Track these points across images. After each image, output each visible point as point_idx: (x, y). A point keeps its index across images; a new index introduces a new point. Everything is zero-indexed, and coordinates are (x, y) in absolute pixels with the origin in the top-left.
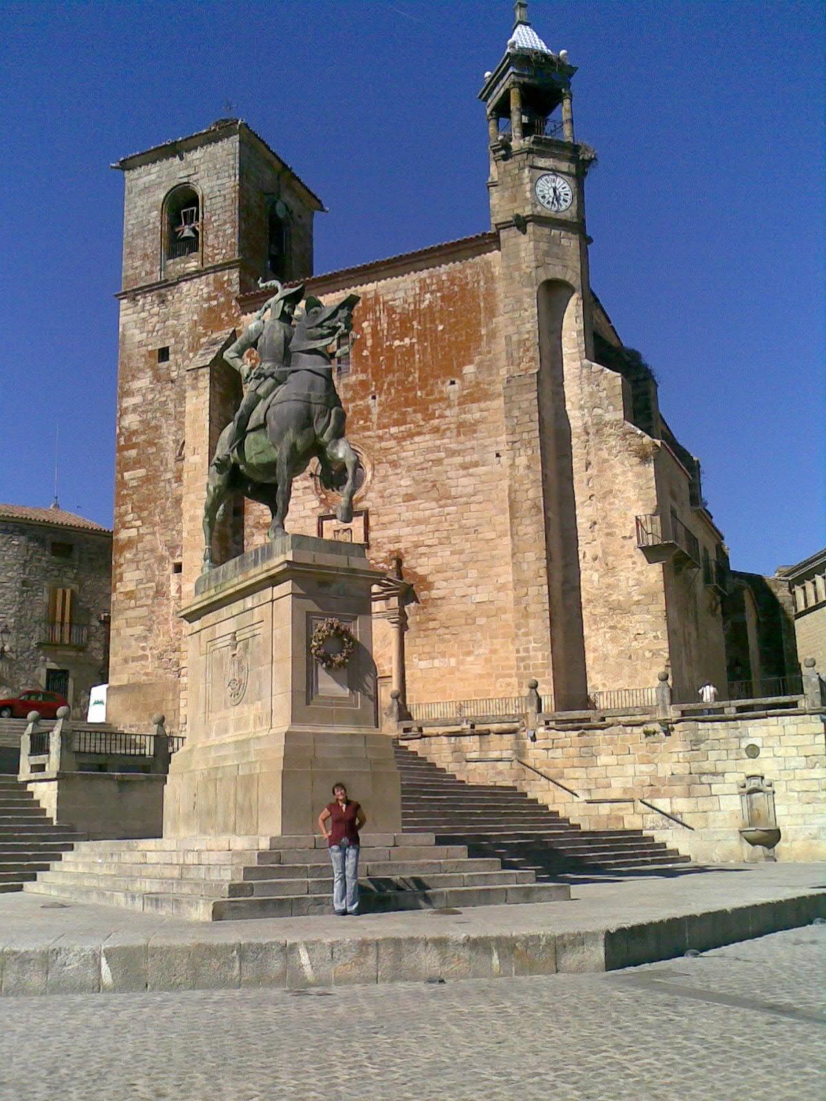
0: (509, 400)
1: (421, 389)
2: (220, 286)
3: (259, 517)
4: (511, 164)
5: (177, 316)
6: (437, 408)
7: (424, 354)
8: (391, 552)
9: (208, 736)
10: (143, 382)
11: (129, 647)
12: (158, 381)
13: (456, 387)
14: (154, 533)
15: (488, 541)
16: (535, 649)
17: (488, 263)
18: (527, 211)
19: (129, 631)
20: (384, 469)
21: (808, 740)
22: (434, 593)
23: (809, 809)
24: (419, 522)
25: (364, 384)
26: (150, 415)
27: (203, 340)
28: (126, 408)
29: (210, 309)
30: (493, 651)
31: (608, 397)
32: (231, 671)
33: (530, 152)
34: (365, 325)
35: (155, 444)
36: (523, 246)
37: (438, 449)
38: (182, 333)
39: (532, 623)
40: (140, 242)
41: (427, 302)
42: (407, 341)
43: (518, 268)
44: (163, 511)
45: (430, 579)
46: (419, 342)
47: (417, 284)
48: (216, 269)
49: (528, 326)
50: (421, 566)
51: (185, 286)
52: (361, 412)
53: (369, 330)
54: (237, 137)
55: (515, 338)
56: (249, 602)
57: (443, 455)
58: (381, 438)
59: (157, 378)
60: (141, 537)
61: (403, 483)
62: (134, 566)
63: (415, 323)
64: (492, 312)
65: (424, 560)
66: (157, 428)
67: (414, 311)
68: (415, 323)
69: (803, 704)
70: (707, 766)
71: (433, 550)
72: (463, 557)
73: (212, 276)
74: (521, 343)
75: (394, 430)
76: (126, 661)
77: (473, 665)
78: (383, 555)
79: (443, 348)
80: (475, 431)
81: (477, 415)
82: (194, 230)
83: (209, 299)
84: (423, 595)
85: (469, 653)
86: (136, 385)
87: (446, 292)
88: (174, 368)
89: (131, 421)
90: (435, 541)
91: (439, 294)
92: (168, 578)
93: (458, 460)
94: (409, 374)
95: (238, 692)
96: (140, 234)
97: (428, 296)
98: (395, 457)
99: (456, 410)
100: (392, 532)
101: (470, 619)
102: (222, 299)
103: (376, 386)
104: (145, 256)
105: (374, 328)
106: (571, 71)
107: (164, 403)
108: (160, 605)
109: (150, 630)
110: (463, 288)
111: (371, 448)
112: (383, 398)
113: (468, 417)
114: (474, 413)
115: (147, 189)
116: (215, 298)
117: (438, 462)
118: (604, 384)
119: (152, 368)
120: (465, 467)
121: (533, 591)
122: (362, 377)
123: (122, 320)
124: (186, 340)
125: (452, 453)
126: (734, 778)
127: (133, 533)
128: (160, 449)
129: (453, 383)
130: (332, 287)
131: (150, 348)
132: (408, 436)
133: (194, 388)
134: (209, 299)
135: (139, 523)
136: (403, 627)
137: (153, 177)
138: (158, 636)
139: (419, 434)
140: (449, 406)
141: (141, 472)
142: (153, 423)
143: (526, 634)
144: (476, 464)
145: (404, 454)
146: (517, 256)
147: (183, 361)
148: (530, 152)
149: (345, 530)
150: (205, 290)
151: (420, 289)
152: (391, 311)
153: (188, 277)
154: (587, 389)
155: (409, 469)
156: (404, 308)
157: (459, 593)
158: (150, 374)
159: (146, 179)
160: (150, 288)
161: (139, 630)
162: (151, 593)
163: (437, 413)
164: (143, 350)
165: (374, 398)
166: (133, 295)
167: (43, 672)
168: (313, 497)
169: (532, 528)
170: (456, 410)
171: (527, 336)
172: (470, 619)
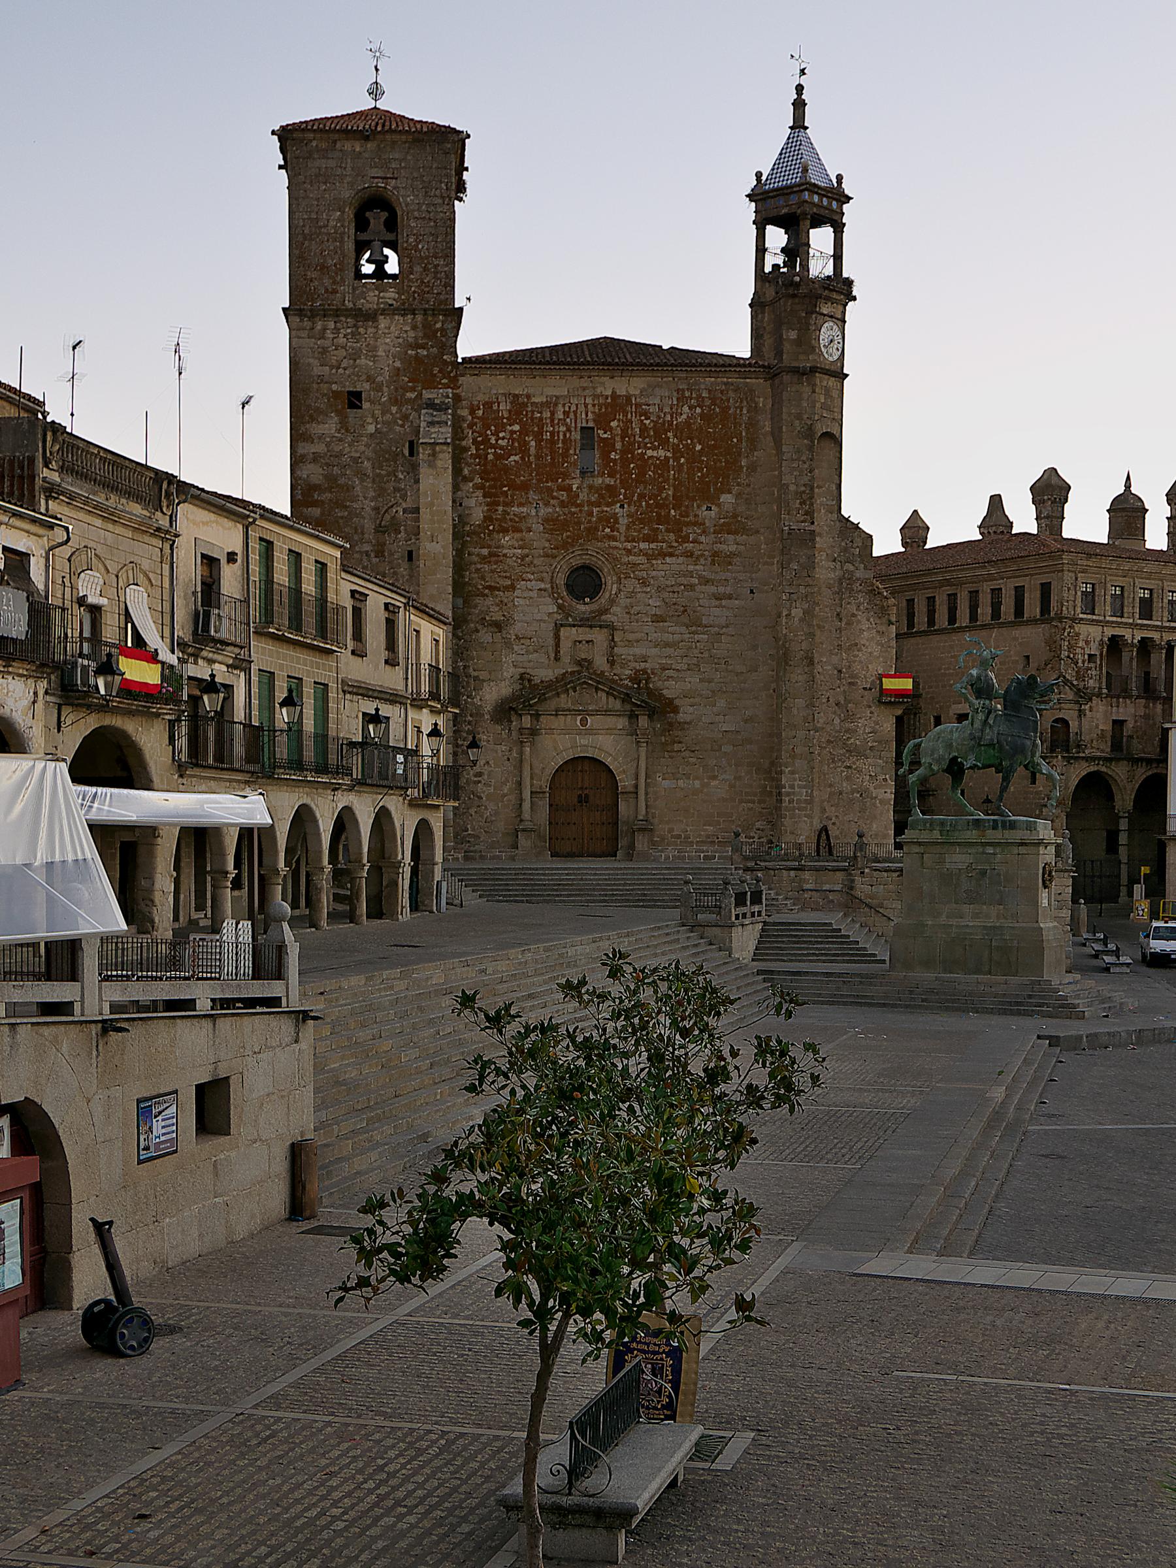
2: (429, 332)
6: (692, 532)
15: (737, 674)
16: (800, 787)
20: (630, 584)
22: (681, 717)
24: (667, 645)
28: (303, 456)
34: (614, 424)
35: (346, 507)
36: (805, 396)
38: (380, 379)
39: (798, 763)
41: (684, 416)
45: (677, 702)
47: (675, 394)
51: (383, 322)
58: (629, 552)
59: (344, 426)
66: (349, 488)
75: (643, 545)
78: (628, 672)
80: (730, 563)
81: (733, 548)
83: (418, 346)
85: (714, 778)
86: (316, 429)
88: (370, 420)
89: (314, 473)
91: (698, 410)
93: (713, 589)
100: (638, 651)
103: (625, 494)
104: (323, 268)
107: (355, 460)
112: (633, 509)
114: (729, 545)
117: (691, 587)
120: (718, 597)
122: (609, 481)
124: (385, 389)
125: (707, 582)
129: (709, 509)
131: (334, 387)
132: (659, 554)
133: (432, 465)
139: (671, 555)
142: (342, 481)
143: (792, 772)
147: (383, 414)
149: (588, 642)
150: (412, 334)
151: (678, 399)
153: (389, 311)
155: (659, 589)
156: (659, 417)
165: (622, 506)
171: (803, 489)
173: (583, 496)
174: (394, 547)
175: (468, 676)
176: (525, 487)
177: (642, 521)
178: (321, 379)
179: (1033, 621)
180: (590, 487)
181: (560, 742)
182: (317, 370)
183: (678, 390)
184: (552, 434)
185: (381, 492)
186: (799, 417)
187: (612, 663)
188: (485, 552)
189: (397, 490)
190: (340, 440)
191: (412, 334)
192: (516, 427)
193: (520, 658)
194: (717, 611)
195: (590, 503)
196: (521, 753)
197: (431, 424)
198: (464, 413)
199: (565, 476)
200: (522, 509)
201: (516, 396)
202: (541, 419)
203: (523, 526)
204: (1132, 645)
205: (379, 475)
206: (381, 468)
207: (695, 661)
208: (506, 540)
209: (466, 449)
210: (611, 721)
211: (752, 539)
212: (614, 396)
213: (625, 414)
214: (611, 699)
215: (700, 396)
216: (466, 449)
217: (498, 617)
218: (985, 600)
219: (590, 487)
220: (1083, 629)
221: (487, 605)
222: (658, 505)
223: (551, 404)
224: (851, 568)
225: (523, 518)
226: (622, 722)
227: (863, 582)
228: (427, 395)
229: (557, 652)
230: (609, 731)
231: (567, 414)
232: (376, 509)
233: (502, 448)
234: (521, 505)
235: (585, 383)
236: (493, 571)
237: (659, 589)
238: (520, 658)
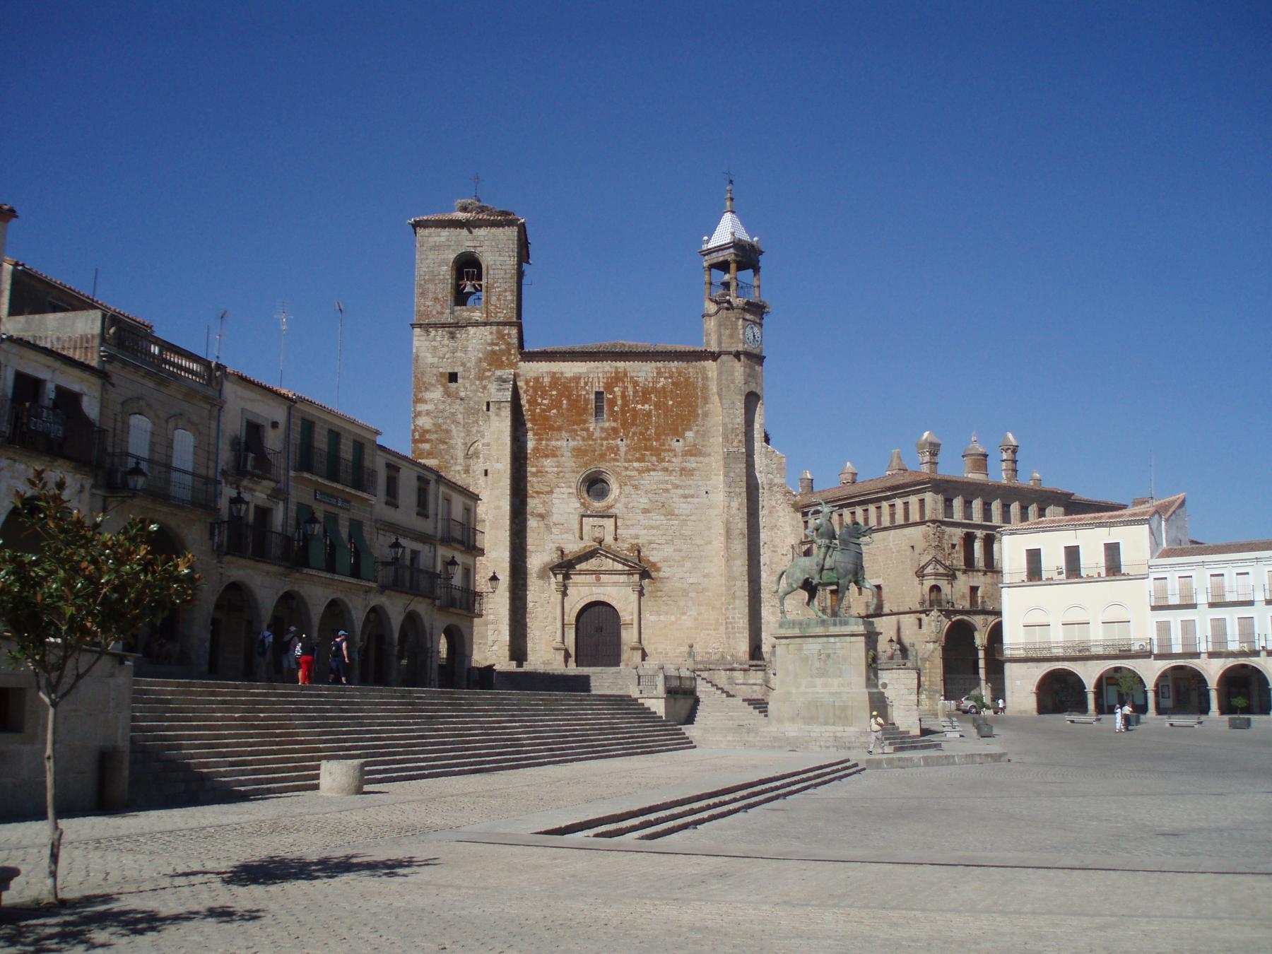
0: (726, 466)
2: (501, 336)
4: (731, 314)
5: (466, 352)
7: (658, 416)
8: (633, 545)
10: (436, 394)
13: (681, 443)
17: (704, 368)
18: (740, 348)
20: (628, 489)
22: (661, 574)
24: (652, 528)
25: (615, 430)
27: (488, 374)
29: (493, 352)
30: (700, 614)
32: (817, 664)
33: (743, 309)
37: (667, 482)
39: (737, 602)
40: (431, 287)
42: (647, 406)
43: (733, 382)
45: (659, 565)
46: (656, 409)
48: (498, 324)
49: (738, 420)
50: (653, 556)
51: (472, 330)
54: (516, 229)
55: (730, 426)
56: (832, 640)
57: (670, 487)
58: (626, 469)
64: (706, 400)
65: (655, 552)
66: (447, 431)
67: (653, 388)
69: (909, 664)
72: (682, 554)
73: (494, 328)
74: (733, 429)
75: (636, 464)
77: (687, 621)
81: (694, 465)
82: (474, 286)
83: (492, 344)
84: (654, 574)
85: (684, 614)
86: (428, 395)
89: (425, 422)
93: (680, 492)
94: (647, 429)
95: (823, 673)
96: (431, 281)
99: (679, 459)
100: (633, 532)
101: (685, 593)
104: (436, 299)
105: (623, 393)
106: (761, 253)
107: (453, 414)
110: (687, 379)
111: (618, 474)
113: (688, 465)
114: (692, 463)
115: (437, 248)
116: (497, 344)
117: (667, 491)
118: (775, 460)
119: (443, 385)
120: (685, 497)
121: (739, 583)
123: (416, 343)
125: (677, 487)
134: (492, 344)
136: (641, 594)
137: (443, 239)
142: (444, 427)
144: (692, 496)
148: (743, 309)
150: (489, 337)
152: (636, 384)
153: (477, 324)
154: (765, 461)
155: (646, 492)
157: (678, 576)
158: (441, 389)
159: (437, 239)
160: (443, 326)
164: (435, 371)
166: (426, 327)
168: (574, 500)
169: (740, 546)
170: (679, 459)
172: (685, 593)
173: (597, 434)
176: (559, 429)
181: (582, 591)
182: (431, 360)
185: (469, 433)
187: (616, 539)
188: (534, 470)
189: (478, 432)
191: (489, 337)
194: (684, 506)
195: (602, 439)
197: (499, 390)
199: (585, 422)
201: (555, 373)
203: (558, 453)
208: (548, 463)
211: (706, 460)
212: (617, 373)
217: (542, 511)
219: (602, 429)
223: (577, 379)
225: (558, 448)
227: (781, 486)
228: (498, 373)
230: (615, 584)
231: (586, 384)
232: (465, 444)
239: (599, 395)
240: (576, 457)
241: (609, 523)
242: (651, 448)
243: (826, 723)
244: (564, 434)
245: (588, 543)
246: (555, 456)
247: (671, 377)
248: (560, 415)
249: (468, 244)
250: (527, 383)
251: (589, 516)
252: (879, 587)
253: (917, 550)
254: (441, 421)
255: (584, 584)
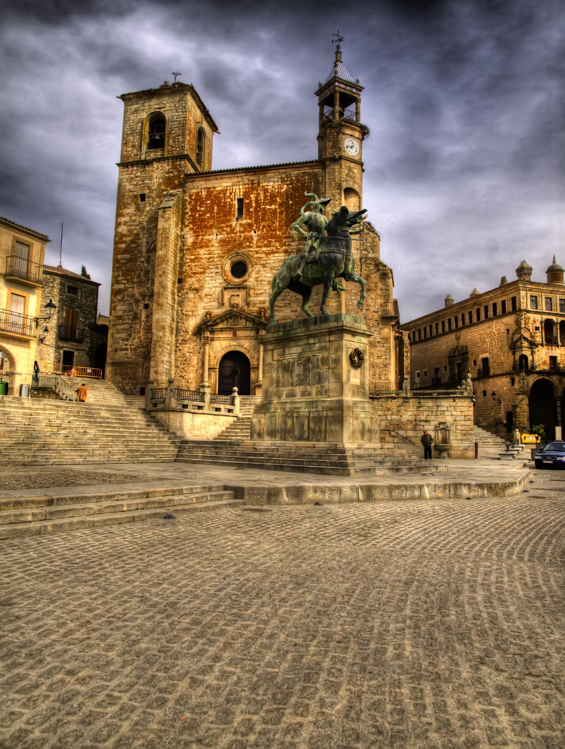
1: (279, 231)
2: (174, 167)
3: (192, 285)
5: (151, 178)
8: (260, 308)
9: (280, 398)
10: (131, 210)
11: (118, 343)
12: (139, 211)
14: (133, 288)
19: (118, 336)
20: (257, 268)
21: (465, 409)
23: (465, 437)
25: (250, 225)
26: (133, 227)
27: (165, 193)
28: (120, 223)
29: (169, 178)
31: (370, 246)
34: (252, 196)
36: (337, 170)
40: (131, 138)
42: (273, 207)
44: (139, 276)
46: (279, 208)
51: (155, 165)
52: (248, 239)
53: (254, 199)
58: (257, 252)
59: (138, 209)
60: (126, 289)
61: (268, 275)
62: (122, 303)
63: (278, 198)
68: (278, 198)
70: (423, 418)
71: (282, 309)
75: (264, 249)
76: (116, 350)
78: (256, 309)
79: (291, 212)
82: (160, 136)
86: (126, 211)
87: (294, 185)
89: (123, 229)
90: (283, 305)
92: (141, 310)
94: (274, 223)
96: (132, 134)
97: (285, 186)
98: (264, 262)
99: (296, 243)
100: (261, 298)
102: (176, 173)
108: (135, 324)
109: (130, 335)
111: (252, 257)
112: (260, 233)
116: (171, 173)
119: (136, 204)
122: (249, 221)
126: (434, 423)
127: (122, 286)
128: (139, 245)
130: (236, 175)
133: (163, 217)
134: (169, 172)
135: (125, 282)
138: (134, 339)
139: (277, 252)
140: (293, 241)
141: (127, 256)
145: (269, 262)
146: (334, 175)
149: (237, 295)
150: (167, 168)
152: (266, 191)
153: (158, 160)
155: (271, 269)
161: (124, 335)
162: (131, 317)
163: (287, 243)
167: (62, 352)
168: (220, 277)
173: (238, 229)
174: (153, 258)
175: (183, 314)
176: (211, 227)
177: (264, 238)
178: (130, 191)
179: (510, 314)
180: (241, 224)
182: (128, 186)
183: (281, 178)
184: (224, 203)
186: (334, 181)
187: (248, 304)
188: (193, 257)
190: (135, 215)
191: (167, 168)
192: (209, 202)
193: (207, 305)
195: (240, 232)
196: (204, 349)
198: (187, 198)
199: (230, 220)
200: (211, 237)
201: (209, 188)
202: (219, 197)
203: (210, 244)
204: (557, 323)
205: (150, 228)
206: (151, 224)
207: (288, 302)
209: (187, 213)
210: (247, 333)
212: (253, 184)
213: (257, 190)
214: (248, 323)
215: (291, 180)
216: (187, 213)
217: (197, 286)
218: (491, 308)
219: (241, 224)
220: (532, 316)
221: (191, 281)
222: (271, 230)
223: (224, 191)
224: (366, 252)
225: (210, 241)
226: (252, 333)
229: (222, 300)
230: (246, 337)
231: (231, 194)
232: (148, 242)
233: (202, 211)
234: (209, 235)
235: (239, 179)
236: (196, 266)
237: (271, 269)
238: (207, 305)
239: (240, 201)
240: (222, 246)
241: (242, 293)
242: (276, 237)
243: (301, 438)
244: (214, 231)
245: (226, 308)
246: (208, 246)
247: (291, 184)
248: (212, 217)
249: (156, 107)
250: (191, 196)
251: (231, 288)
252: (485, 360)
253: (511, 333)
254: (133, 227)
255: (225, 339)
